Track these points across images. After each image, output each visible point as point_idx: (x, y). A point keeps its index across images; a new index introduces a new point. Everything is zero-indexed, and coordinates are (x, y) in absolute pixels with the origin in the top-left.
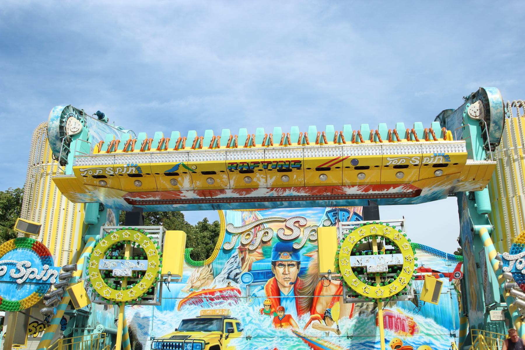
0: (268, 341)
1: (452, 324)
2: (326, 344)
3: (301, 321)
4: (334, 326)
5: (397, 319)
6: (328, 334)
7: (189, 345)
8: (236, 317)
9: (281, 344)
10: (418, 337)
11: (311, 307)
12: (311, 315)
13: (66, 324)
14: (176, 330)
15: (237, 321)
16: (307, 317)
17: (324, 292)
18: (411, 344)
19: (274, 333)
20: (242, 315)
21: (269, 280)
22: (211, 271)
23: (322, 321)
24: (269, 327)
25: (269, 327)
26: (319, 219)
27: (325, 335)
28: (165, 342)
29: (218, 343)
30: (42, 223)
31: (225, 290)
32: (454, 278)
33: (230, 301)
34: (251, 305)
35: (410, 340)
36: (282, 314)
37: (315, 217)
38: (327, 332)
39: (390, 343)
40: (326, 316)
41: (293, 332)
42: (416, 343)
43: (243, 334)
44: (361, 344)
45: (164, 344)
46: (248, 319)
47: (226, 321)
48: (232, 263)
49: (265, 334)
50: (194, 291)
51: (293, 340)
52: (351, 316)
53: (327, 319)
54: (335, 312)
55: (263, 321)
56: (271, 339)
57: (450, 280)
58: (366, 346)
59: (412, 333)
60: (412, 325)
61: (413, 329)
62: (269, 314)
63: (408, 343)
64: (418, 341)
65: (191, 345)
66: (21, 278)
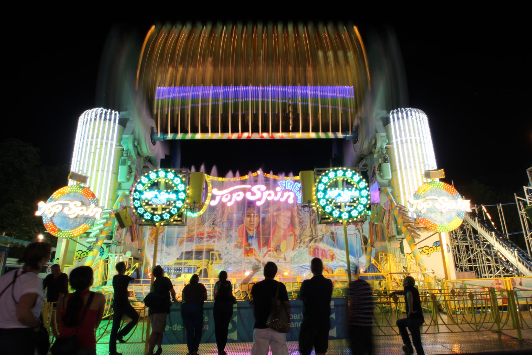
3: (261, 253)
4: (283, 256)
5: (323, 250)
6: (278, 261)
7: (186, 269)
8: (219, 250)
10: (335, 262)
11: (267, 243)
12: (268, 248)
13: (103, 251)
14: (177, 259)
15: (219, 253)
16: (265, 250)
17: (276, 234)
18: (332, 267)
20: (222, 249)
21: (240, 226)
22: (202, 220)
23: (275, 253)
24: (241, 256)
28: (170, 267)
29: (206, 267)
30: (89, 175)
31: (211, 233)
33: (213, 240)
34: (228, 242)
36: (249, 248)
38: (278, 259)
40: (277, 249)
41: (256, 259)
42: (335, 266)
43: (223, 261)
44: (299, 267)
46: (226, 251)
47: (211, 252)
48: (215, 214)
49: (237, 261)
50: (190, 233)
52: (293, 249)
53: (278, 251)
54: (283, 247)
55: (236, 252)
56: (241, 264)
57: (356, 226)
58: (303, 268)
59: (332, 260)
61: (333, 257)
62: (240, 247)
64: (336, 265)
65: (188, 269)
66: (74, 214)
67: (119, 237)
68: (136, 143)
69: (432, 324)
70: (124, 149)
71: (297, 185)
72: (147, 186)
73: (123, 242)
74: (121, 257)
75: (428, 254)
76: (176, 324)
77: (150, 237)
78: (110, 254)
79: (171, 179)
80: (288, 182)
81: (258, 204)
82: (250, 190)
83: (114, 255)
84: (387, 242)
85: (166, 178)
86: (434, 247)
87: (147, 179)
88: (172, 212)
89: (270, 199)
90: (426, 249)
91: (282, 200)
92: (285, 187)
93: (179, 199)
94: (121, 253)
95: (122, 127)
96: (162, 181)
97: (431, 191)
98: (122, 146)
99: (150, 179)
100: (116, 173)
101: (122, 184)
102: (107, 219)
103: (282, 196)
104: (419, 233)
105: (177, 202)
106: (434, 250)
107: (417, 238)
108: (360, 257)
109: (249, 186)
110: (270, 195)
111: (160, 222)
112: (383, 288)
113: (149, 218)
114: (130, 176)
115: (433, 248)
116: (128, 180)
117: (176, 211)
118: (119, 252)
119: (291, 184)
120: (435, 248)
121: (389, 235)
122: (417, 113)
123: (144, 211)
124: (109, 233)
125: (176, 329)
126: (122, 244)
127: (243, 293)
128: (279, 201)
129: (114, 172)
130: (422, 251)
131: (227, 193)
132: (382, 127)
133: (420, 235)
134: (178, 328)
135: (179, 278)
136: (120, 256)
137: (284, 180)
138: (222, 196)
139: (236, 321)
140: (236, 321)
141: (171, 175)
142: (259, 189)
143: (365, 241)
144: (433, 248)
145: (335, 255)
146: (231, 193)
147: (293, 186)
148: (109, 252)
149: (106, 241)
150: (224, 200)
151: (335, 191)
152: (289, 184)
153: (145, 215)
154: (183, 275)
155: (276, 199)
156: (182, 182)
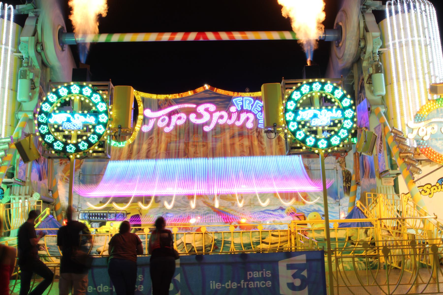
0: (182, 210)
1: (337, 194)
2: (232, 212)
7: (112, 215)
9: (194, 212)
13: (4, 193)
18: (303, 211)
19: (187, 204)
25: (182, 198)
26: (226, 106)
27: (231, 205)
28: (91, 213)
32: (340, 157)
35: (302, 208)
37: (223, 104)
39: (286, 211)
41: (205, 202)
42: (308, 210)
44: (261, 211)
45: (90, 214)
51: (203, 209)
56: (184, 209)
57: (337, 158)
58: (266, 213)
60: (305, 196)
63: (301, 210)
64: (309, 209)
65: (114, 215)
67: (22, 174)
68: (39, 48)
69: (431, 282)
70: (23, 56)
71: (257, 103)
72: (57, 106)
73: (28, 180)
74: (26, 200)
75: (430, 194)
76: (102, 285)
77: (63, 174)
78: (12, 197)
79: (87, 96)
80: (246, 100)
81: (207, 129)
82: (194, 111)
83: (17, 198)
84: (377, 178)
85: (81, 95)
86: (438, 185)
87: (55, 97)
88: (91, 139)
89: (221, 122)
90: (427, 188)
91: (238, 124)
92: (242, 106)
93: (99, 123)
94: (26, 195)
95: (19, 27)
96: (76, 99)
97: (438, 111)
98: (20, 52)
99: (59, 97)
100: (14, 90)
101: (23, 104)
102: (5, 150)
103: (238, 118)
104: (420, 167)
105: (97, 127)
106: (438, 189)
107: (417, 173)
108: (341, 198)
109: (194, 106)
110: (222, 117)
111: (76, 154)
112: (370, 237)
113: (60, 148)
114: (33, 94)
115: (437, 187)
116: (31, 98)
117: (96, 139)
118: (23, 194)
119: (250, 102)
120: (440, 187)
121: (380, 170)
122: (422, 5)
123: (54, 140)
124: (9, 169)
125: (101, 291)
126: (27, 184)
127: (188, 245)
128: (233, 125)
129: (12, 88)
130: (423, 190)
131: (163, 115)
132: (375, 23)
133: (420, 170)
134: (104, 289)
135: (104, 227)
136: (26, 198)
137: (241, 96)
138: (158, 118)
139: (179, 280)
140: (179, 280)
141: (87, 91)
142: (207, 110)
143: (348, 177)
144: (437, 187)
145: (308, 196)
146: (170, 115)
147: (252, 105)
148: (10, 194)
149: (5, 180)
150: (160, 124)
151: (310, 111)
152: (248, 102)
153: (55, 144)
154: (108, 223)
155: (230, 122)
156: (103, 100)
